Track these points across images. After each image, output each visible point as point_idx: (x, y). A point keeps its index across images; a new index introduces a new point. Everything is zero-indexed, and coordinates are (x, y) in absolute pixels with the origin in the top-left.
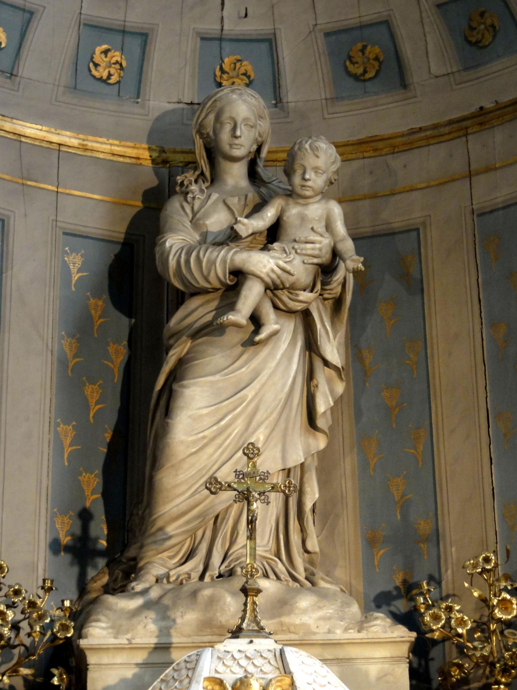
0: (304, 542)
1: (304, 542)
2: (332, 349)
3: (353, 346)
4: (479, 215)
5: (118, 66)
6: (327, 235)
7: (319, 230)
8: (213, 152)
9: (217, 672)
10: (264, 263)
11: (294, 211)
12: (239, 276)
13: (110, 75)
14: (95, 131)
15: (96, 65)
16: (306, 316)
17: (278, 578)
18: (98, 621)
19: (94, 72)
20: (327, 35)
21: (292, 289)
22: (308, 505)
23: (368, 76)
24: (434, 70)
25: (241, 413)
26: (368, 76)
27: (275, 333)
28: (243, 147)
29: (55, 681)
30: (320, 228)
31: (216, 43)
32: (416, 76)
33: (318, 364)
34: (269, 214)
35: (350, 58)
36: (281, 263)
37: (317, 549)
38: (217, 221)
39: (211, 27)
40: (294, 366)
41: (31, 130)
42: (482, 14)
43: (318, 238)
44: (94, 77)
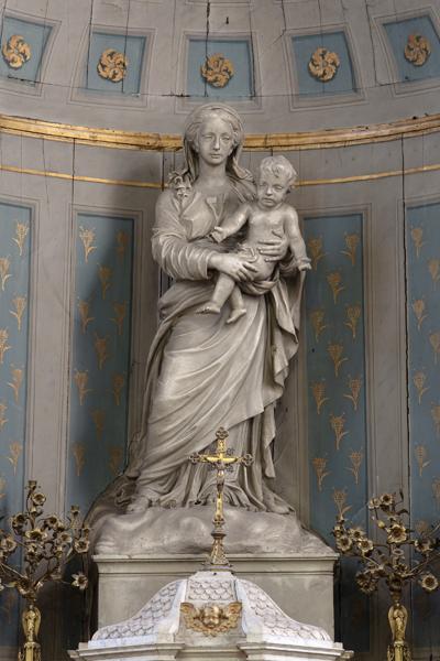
0: (263, 471)
1: (263, 471)
2: (288, 321)
3: (305, 312)
4: (408, 209)
5: (121, 66)
6: (284, 236)
7: (279, 233)
8: (195, 155)
9: (190, 598)
10: (232, 263)
11: (258, 218)
12: (214, 273)
13: (115, 75)
14: (101, 124)
15: (103, 67)
16: (269, 298)
17: (242, 505)
18: (106, 540)
19: (102, 73)
20: (294, 39)
21: (257, 281)
22: (267, 442)
23: (326, 78)
24: (382, 79)
25: (214, 377)
26: (326, 78)
27: (243, 315)
28: (224, 148)
29: (76, 583)
30: (280, 231)
31: (203, 44)
32: (365, 82)
33: (278, 334)
34: (241, 218)
35: (313, 61)
36: (248, 264)
37: (273, 475)
38: (200, 218)
39: (198, 30)
40: (258, 338)
41: (51, 129)
42: (418, 39)
43: (277, 240)
44: (102, 77)
